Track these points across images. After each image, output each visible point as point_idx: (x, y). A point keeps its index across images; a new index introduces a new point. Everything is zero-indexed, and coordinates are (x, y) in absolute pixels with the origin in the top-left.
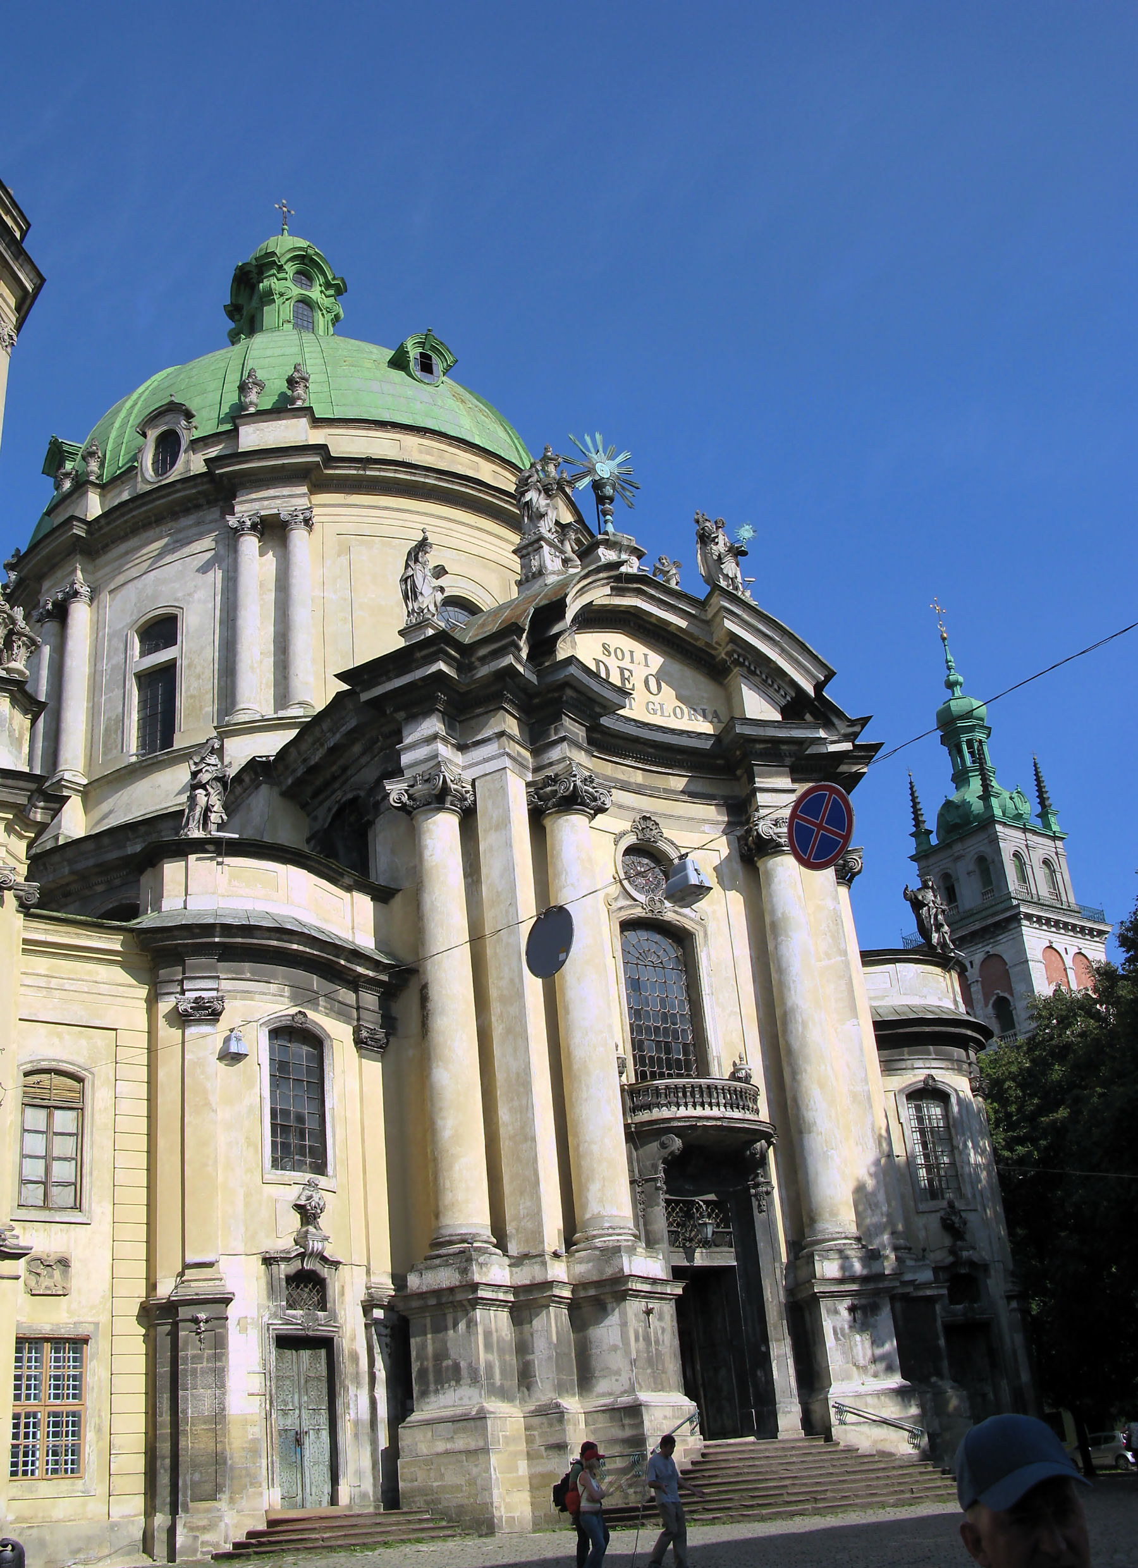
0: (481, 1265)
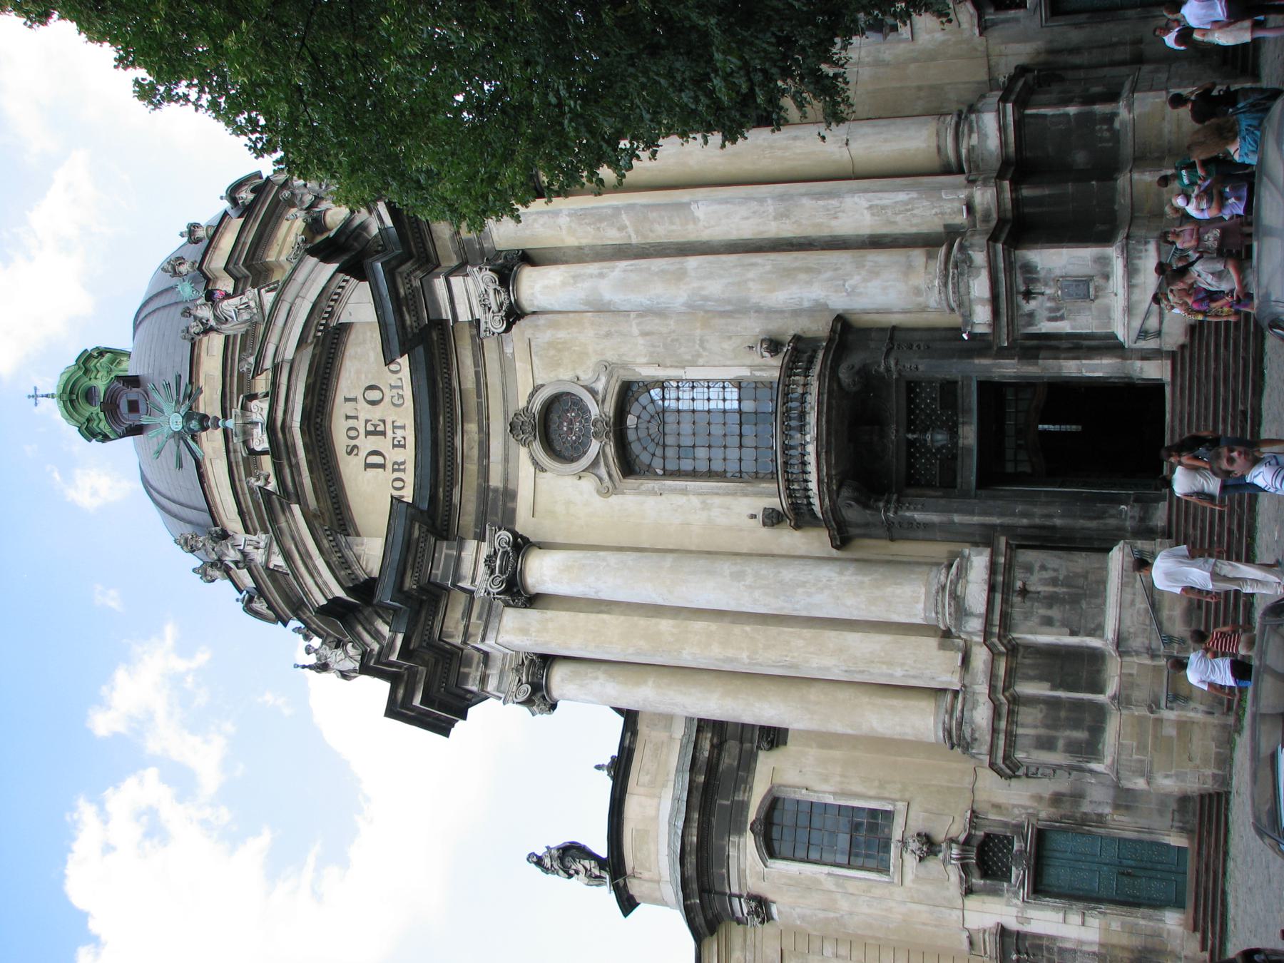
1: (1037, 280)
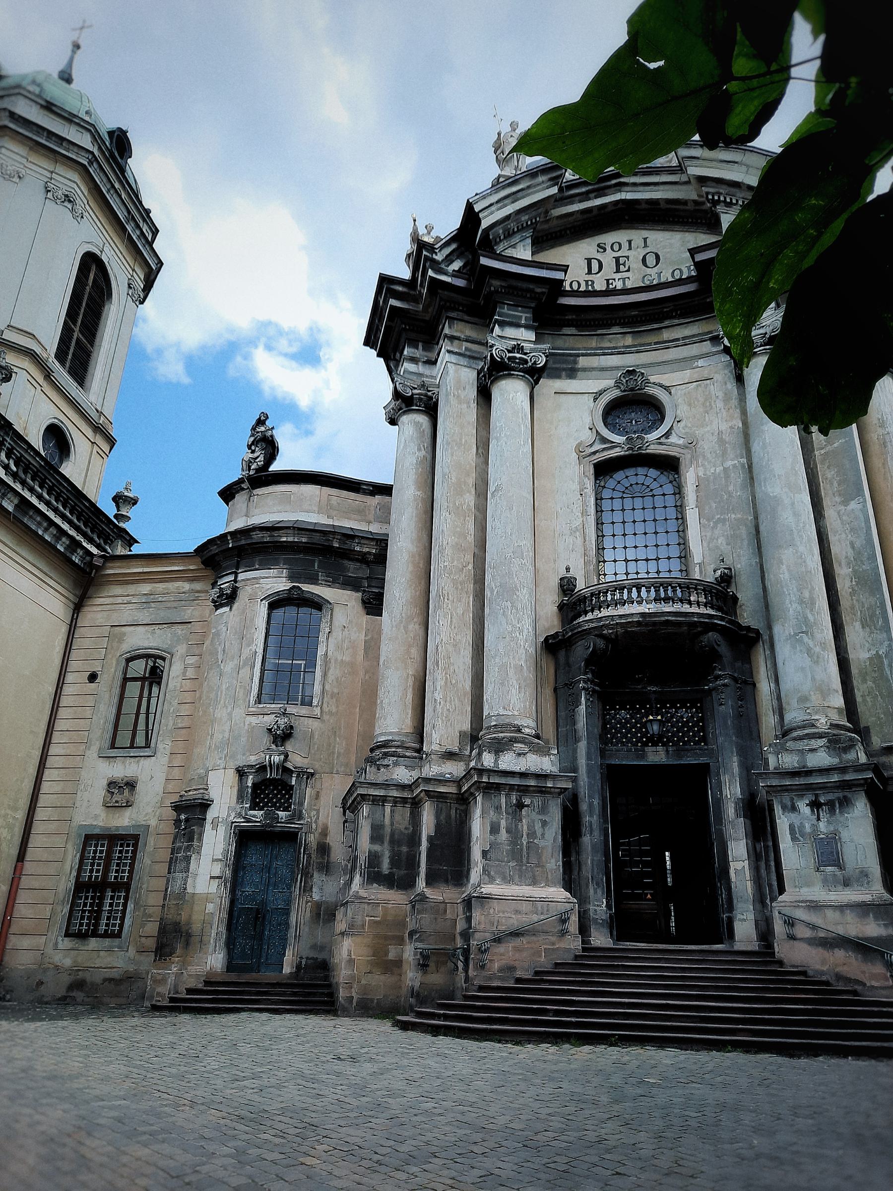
1: (832, 811)
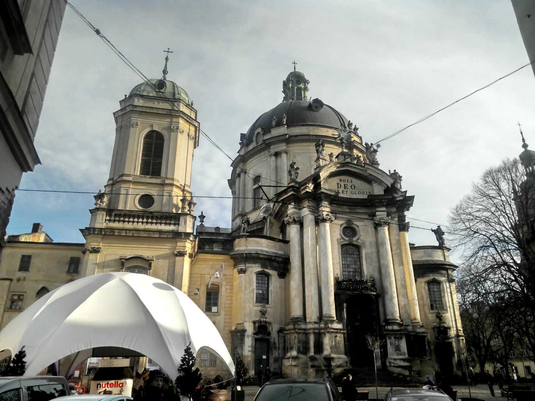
0: (298, 325)
1: (398, 339)
